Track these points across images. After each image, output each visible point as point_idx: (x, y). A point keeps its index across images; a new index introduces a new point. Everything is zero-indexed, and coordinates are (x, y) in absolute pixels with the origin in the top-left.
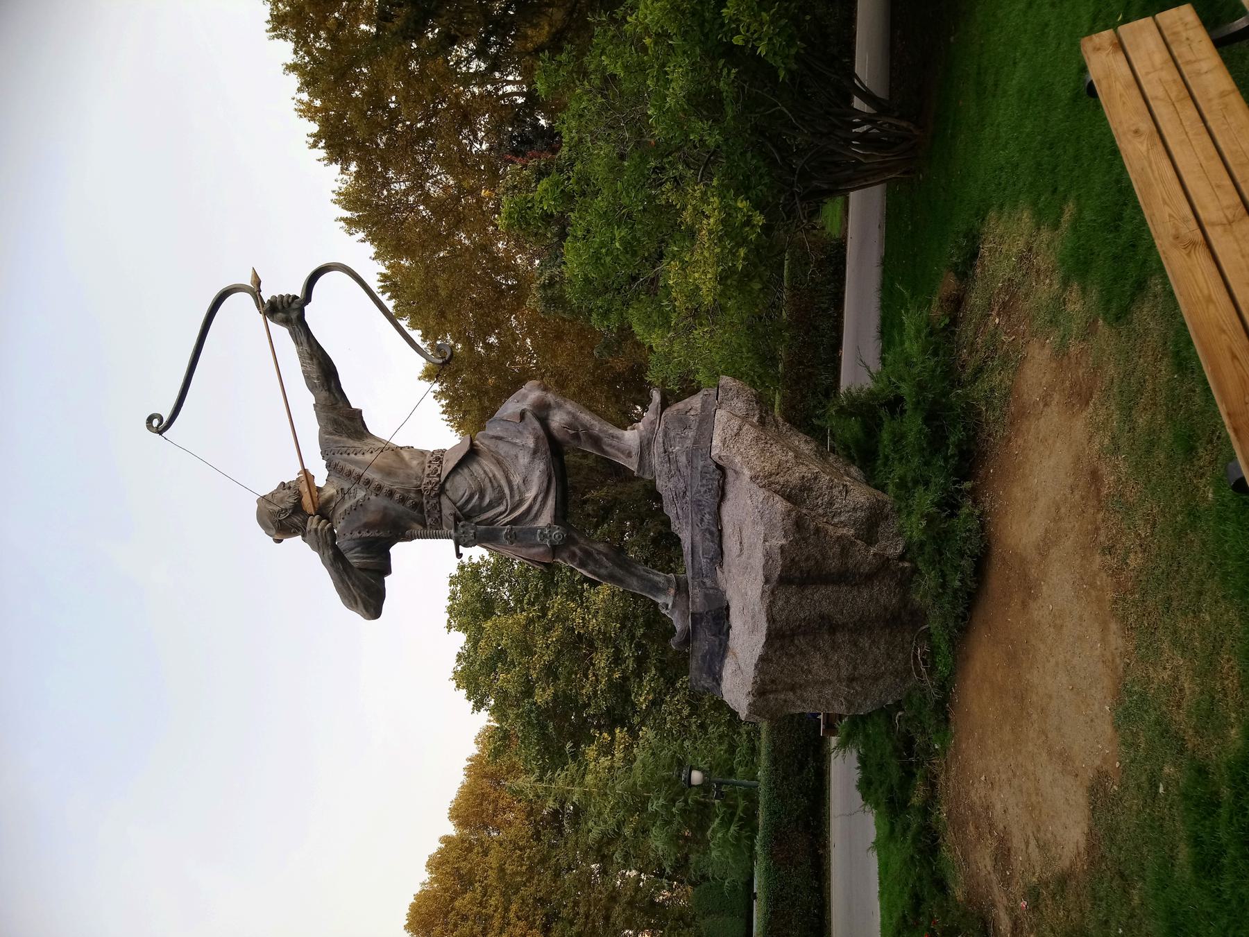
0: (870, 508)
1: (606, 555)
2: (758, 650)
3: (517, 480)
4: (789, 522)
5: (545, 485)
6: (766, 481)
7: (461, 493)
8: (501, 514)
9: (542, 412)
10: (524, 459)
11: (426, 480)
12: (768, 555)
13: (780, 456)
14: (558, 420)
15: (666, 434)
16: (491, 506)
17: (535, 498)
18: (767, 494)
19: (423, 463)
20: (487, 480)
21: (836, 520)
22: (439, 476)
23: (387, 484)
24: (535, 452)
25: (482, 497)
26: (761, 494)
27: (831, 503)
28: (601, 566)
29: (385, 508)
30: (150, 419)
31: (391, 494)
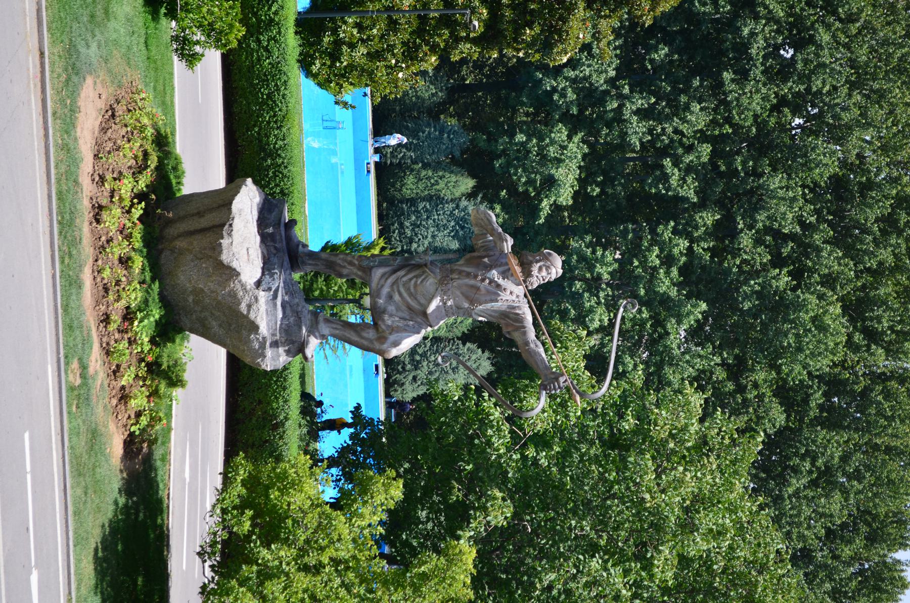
3: (397, 297)
10: (391, 308)
16: (411, 279)
17: (382, 286)
25: (416, 285)
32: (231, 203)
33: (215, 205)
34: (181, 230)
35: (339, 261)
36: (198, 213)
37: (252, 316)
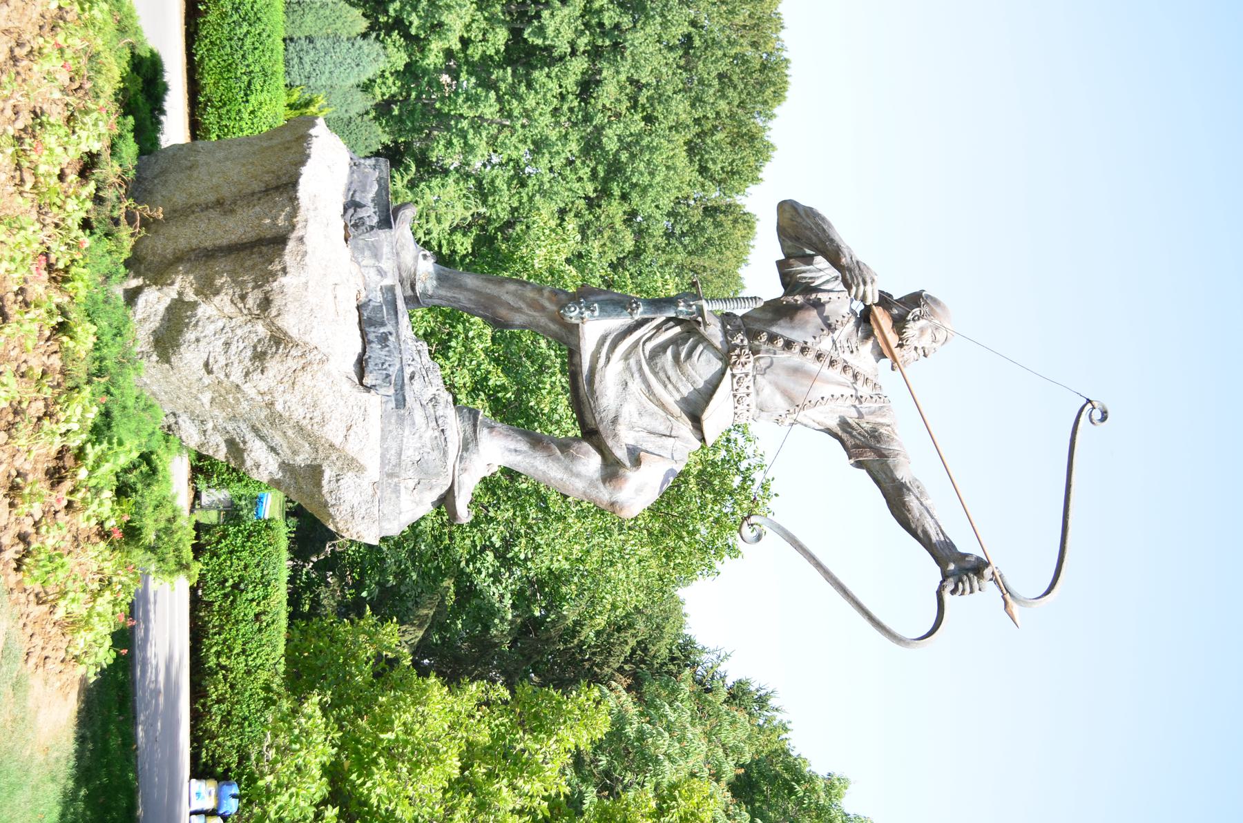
0: (178, 346)
1: (512, 309)
2: (305, 170)
3: (636, 385)
4: (277, 301)
5: (597, 378)
6: (309, 358)
7: (703, 357)
8: (649, 339)
9: (612, 470)
10: (629, 411)
11: (749, 367)
12: (302, 266)
13: (293, 399)
14: (591, 462)
15: (445, 453)
16: (663, 348)
17: (608, 359)
18: (307, 338)
19: (758, 393)
20: (674, 379)
21: (220, 324)
22: (733, 376)
23: (794, 358)
24: (615, 421)
25: (676, 357)
26: (314, 339)
27: (227, 344)
28: (515, 294)
29: (793, 328)
30: (1104, 417)
31: (788, 345)
32: (293, 184)
33: (256, 186)
34: (182, 244)
35: (506, 297)
36: (219, 203)
37: (352, 449)
